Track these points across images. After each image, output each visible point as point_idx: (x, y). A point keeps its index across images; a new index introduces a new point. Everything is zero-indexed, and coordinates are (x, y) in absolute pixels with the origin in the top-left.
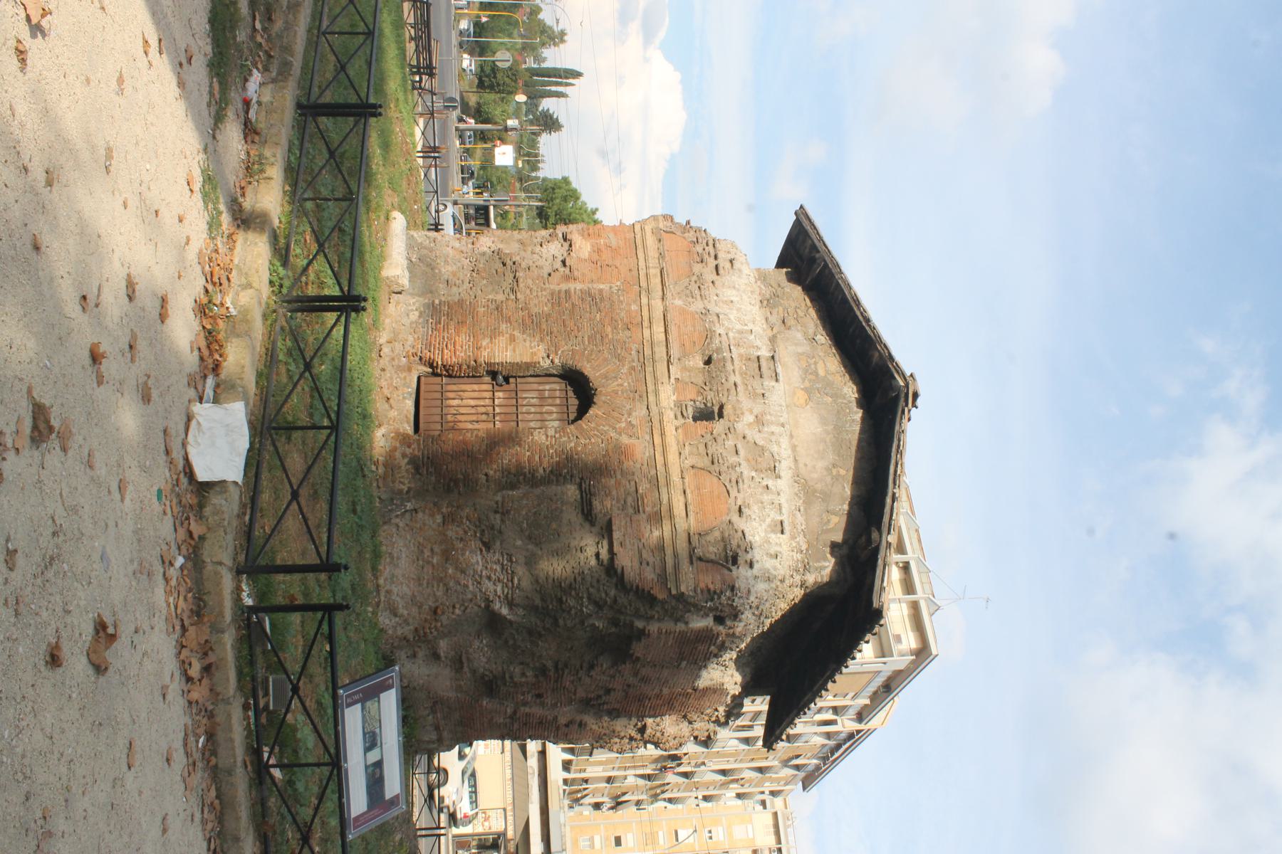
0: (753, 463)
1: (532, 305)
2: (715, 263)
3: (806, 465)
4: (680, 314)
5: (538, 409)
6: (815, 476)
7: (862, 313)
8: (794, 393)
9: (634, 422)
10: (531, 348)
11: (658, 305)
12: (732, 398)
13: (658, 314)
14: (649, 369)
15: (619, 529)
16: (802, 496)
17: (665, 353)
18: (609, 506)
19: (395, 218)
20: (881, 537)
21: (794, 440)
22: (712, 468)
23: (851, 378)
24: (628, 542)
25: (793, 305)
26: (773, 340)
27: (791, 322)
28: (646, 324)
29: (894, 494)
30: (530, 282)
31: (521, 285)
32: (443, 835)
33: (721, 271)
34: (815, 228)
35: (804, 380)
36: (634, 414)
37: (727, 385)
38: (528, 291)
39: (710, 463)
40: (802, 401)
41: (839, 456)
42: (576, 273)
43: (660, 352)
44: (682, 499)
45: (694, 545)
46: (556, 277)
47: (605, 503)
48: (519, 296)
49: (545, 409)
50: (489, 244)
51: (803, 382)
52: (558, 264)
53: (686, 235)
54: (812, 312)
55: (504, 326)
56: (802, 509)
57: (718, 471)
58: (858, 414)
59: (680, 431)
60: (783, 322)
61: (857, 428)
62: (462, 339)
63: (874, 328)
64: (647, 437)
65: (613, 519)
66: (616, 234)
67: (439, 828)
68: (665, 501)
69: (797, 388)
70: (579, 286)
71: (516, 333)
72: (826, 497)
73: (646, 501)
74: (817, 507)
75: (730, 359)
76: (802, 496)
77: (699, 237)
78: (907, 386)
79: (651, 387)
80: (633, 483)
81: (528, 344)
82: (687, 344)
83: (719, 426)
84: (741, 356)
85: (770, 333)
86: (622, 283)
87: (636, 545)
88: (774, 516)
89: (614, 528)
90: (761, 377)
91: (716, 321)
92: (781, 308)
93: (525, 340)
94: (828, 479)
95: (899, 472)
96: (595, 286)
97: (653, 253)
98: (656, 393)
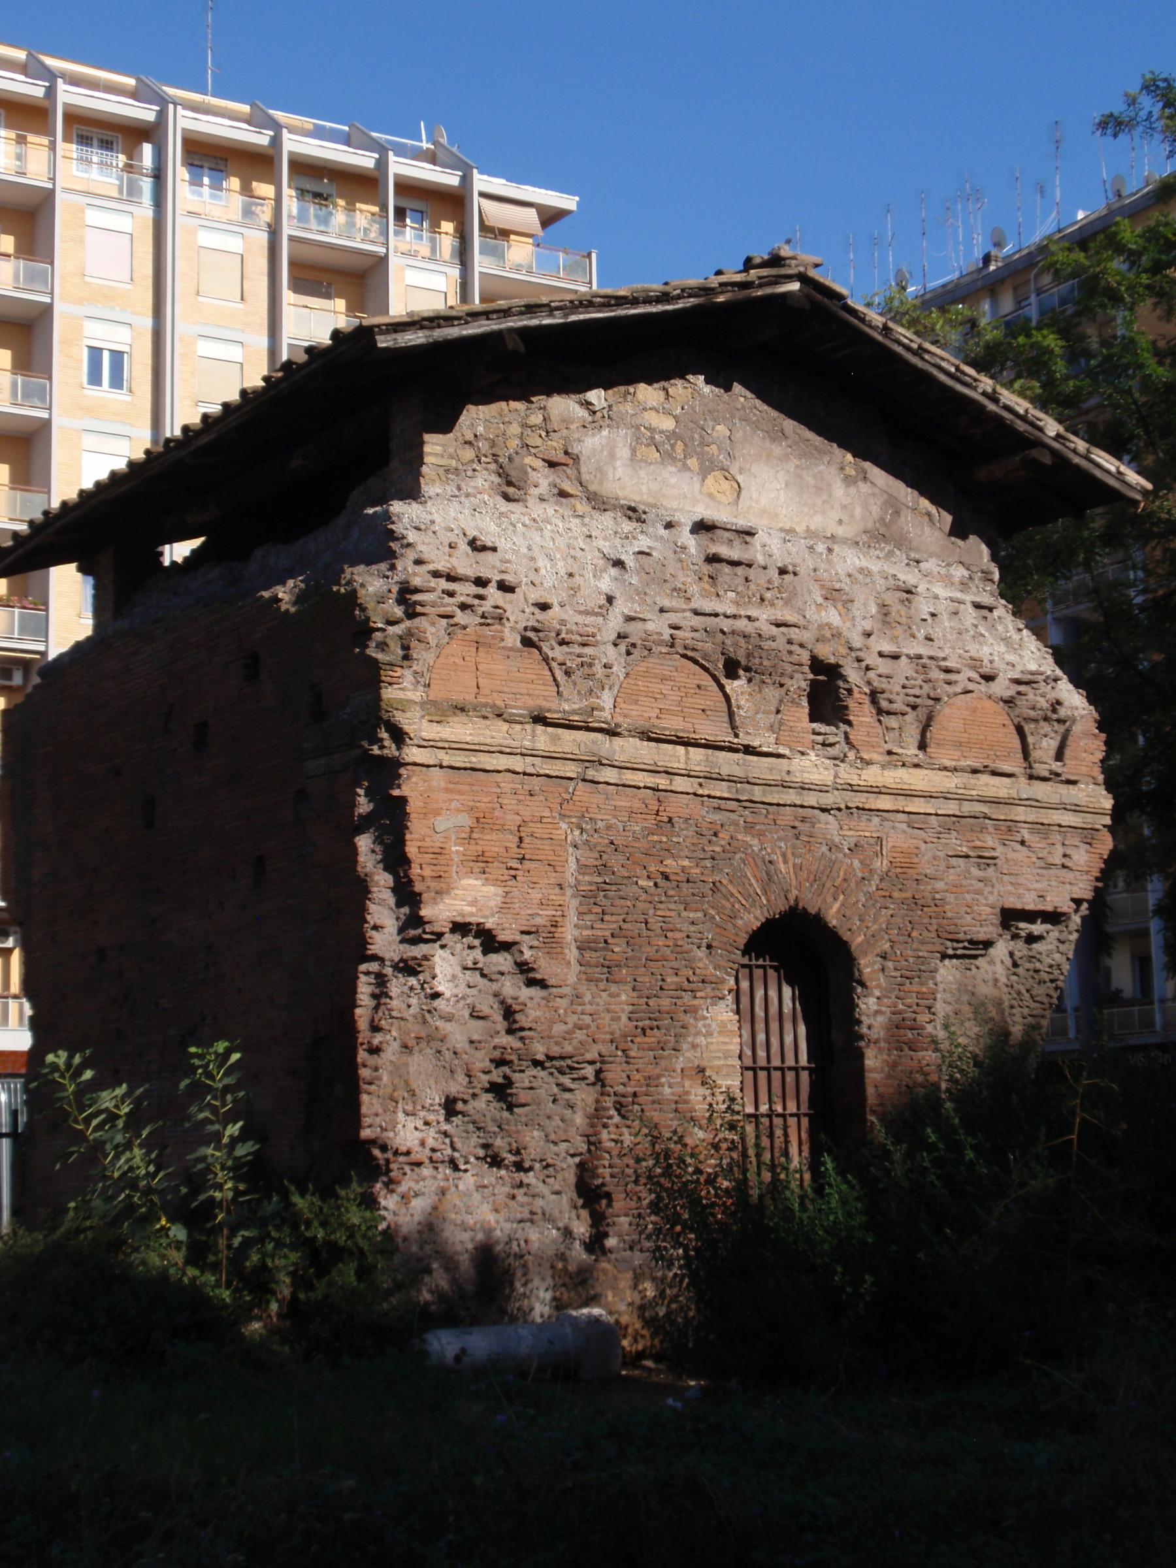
0: (899, 631)
1: (615, 1026)
2: (494, 584)
3: (840, 522)
4: (636, 702)
5: (760, 1026)
6: (858, 511)
8: (710, 496)
9: (853, 841)
10: (709, 1034)
12: (806, 636)
13: (646, 752)
14: (758, 793)
15: (1019, 896)
16: (888, 548)
17: (729, 755)
18: (988, 910)
21: (798, 530)
22: (922, 713)
24: (1038, 886)
26: (599, 503)
28: (662, 782)
29: (984, 394)
30: (559, 1028)
31: (568, 1049)
33: (509, 578)
34: (431, 319)
35: (686, 468)
36: (837, 839)
37: (781, 644)
38: (580, 1035)
39: (915, 713)
40: (726, 485)
41: (825, 453)
42: (539, 921)
43: (727, 762)
44: (985, 778)
45: (1046, 774)
46: (545, 968)
47: (984, 917)
49: (759, 1012)
51: (689, 469)
52: (501, 961)
53: (433, 642)
55: (667, 1090)
56: (913, 555)
57: (931, 702)
59: (866, 756)
60: (552, 464)
63: (683, 290)
64: (876, 820)
65: (1007, 906)
66: (437, 812)
68: (985, 809)
69: (702, 485)
70: (572, 917)
71: (680, 1063)
72: (894, 506)
73: (978, 843)
75: (730, 621)
76: (888, 548)
77: (442, 610)
78: (802, 278)
79: (791, 797)
80: (954, 861)
81: (701, 1040)
82: (702, 703)
83: (853, 675)
84: (704, 595)
85: (582, 507)
86: (562, 816)
87: (1040, 871)
88: (970, 615)
89: (1019, 906)
90: (750, 566)
91: (639, 625)
92: (528, 460)
93: (694, 1046)
94: (864, 487)
95: (953, 370)
96: (572, 881)
97: (497, 733)
98: (804, 788)
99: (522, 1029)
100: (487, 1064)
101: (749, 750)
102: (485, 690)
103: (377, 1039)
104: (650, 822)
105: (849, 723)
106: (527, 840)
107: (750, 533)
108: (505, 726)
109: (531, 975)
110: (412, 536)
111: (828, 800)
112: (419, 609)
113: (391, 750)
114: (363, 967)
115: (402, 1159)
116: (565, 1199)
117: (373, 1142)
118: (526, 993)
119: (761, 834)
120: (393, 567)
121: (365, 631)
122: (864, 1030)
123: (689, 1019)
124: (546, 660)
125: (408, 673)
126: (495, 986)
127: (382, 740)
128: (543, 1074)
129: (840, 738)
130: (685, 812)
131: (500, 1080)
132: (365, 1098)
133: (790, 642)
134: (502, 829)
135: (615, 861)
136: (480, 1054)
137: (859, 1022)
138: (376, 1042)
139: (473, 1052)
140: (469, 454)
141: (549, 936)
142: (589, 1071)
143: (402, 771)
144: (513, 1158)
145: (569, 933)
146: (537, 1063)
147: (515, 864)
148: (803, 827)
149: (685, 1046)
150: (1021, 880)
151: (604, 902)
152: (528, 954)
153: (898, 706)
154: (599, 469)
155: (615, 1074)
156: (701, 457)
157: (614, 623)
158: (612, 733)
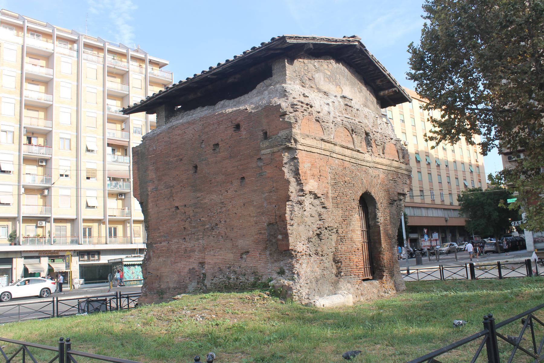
4: (337, 138)
7: (333, 41)
11: (338, 149)
14: (359, 162)
19: (323, 306)
20: (397, 88)
23: (329, 59)
25: (302, 70)
26: (319, 90)
27: (309, 75)
31: (332, 225)
32: (57, 299)
34: (296, 37)
38: (333, 221)
40: (340, 90)
42: (325, 192)
43: (355, 154)
48: (336, 227)
50: (301, 245)
52: (317, 202)
54: (306, 61)
58: (340, 66)
60: (310, 79)
61: (346, 70)
62: (355, 259)
67: (53, 301)
70: (330, 191)
72: (366, 99)
74: (369, 104)
78: (359, 42)
79: (364, 163)
81: (354, 223)
85: (316, 91)
99: (323, 220)
100: (316, 229)
101: (358, 151)
102: (311, 132)
103: (292, 222)
104: (342, 168)
105: (372, 147)
106: (321, 171)
107: (352, 100)
108: (316, 141)
109: (323, 206)
110: (291, 92)
111: (371, 165)
112: (297, 110)
113: (294, 146)
114: (287, 203)
115: (299, 254)
116: (330, 263)
117: (292, 250)
118: (323, 210)
119: (360, 172)
120: (287, 99)
121: (285, 114)
122: (379, 221)
123: (351, 217)
124: (321, 125)
125: (297, 125)
126: (316, 208)
127: (291, 143)
128: (326, 231)
129: (370, 150)
130: (347, 166)
131: (319, 233)
132: (290, 238)
133: (361, 126)
134: (316, 168)
135: (337, 177)
136: (314, 226)
137: (378, 219)
138: (292, 223)
139: (313, 225)
140: (295, 75)
141: (326, 195)
142: (335, 230)
143: (297, 151)
144: (321, 253)
145: (330, 195)
146: (326, 228)
147: (319, 177)
148: (367, 171)
149: (351, 224)
150: (400, 186)
151: (336, 188)
152: (323, 200)
153: (379, 144)
154: (318, 82)
155: (340, 231)
156: (335, 82)
157: (331, 119)
158: (335, 145)
